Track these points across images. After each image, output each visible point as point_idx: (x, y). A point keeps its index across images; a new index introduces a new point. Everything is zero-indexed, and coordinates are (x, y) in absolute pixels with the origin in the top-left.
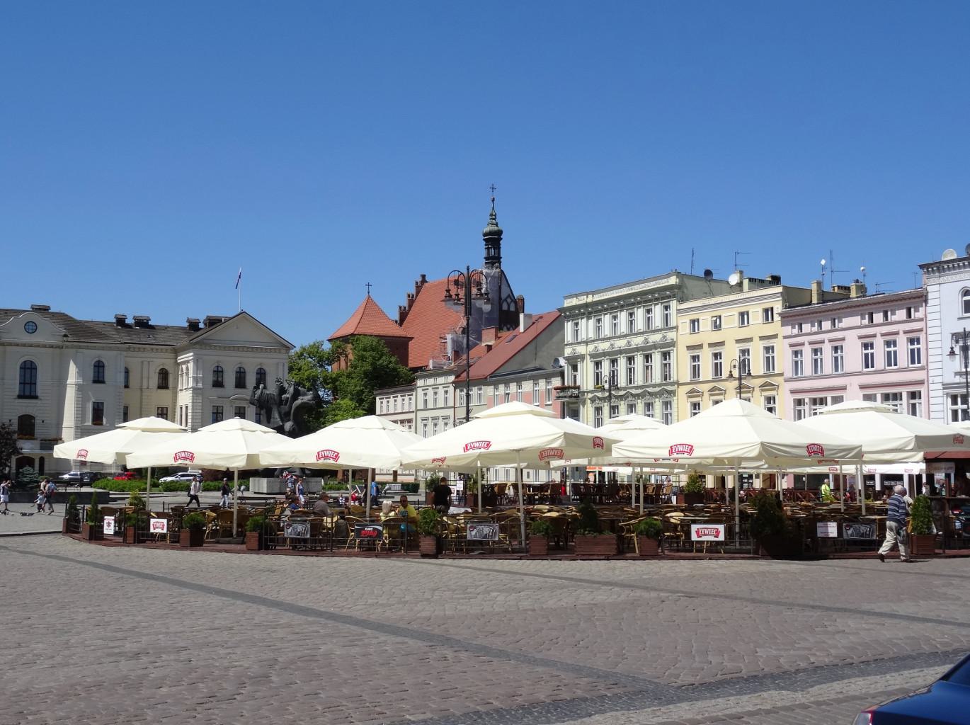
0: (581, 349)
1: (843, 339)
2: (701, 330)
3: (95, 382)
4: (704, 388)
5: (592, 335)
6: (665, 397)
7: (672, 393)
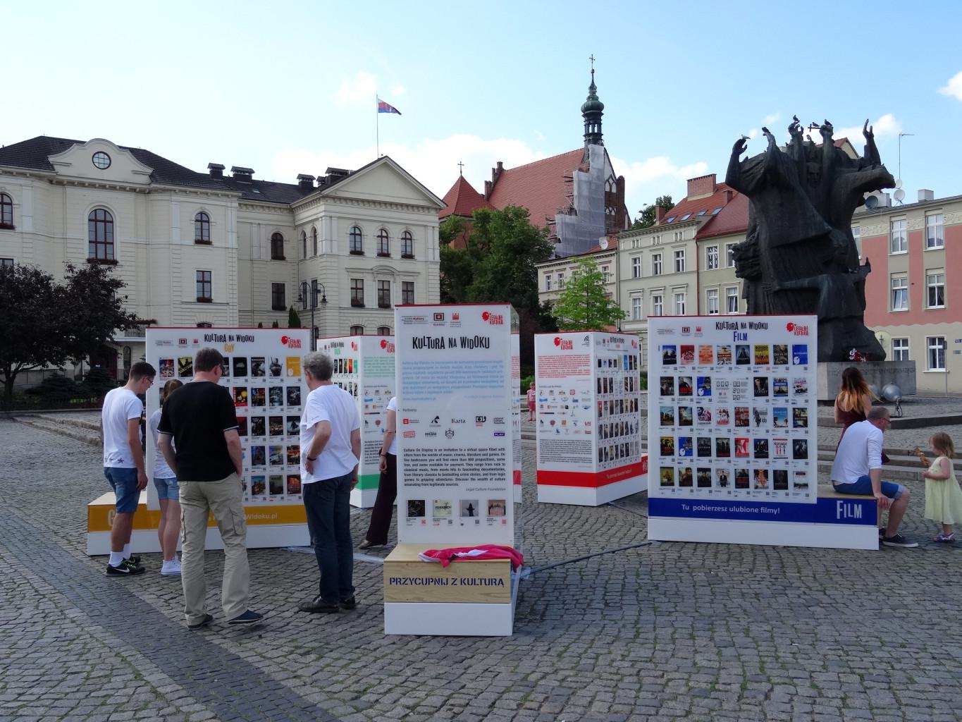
3: (199, 242)
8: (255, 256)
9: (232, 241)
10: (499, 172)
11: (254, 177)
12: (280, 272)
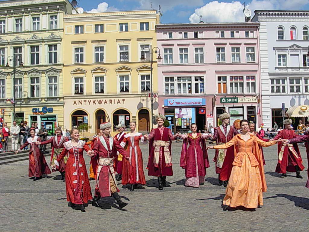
2: (85, 31)
4: (89, 69)
6: (51, 74)
7: (60, 71)
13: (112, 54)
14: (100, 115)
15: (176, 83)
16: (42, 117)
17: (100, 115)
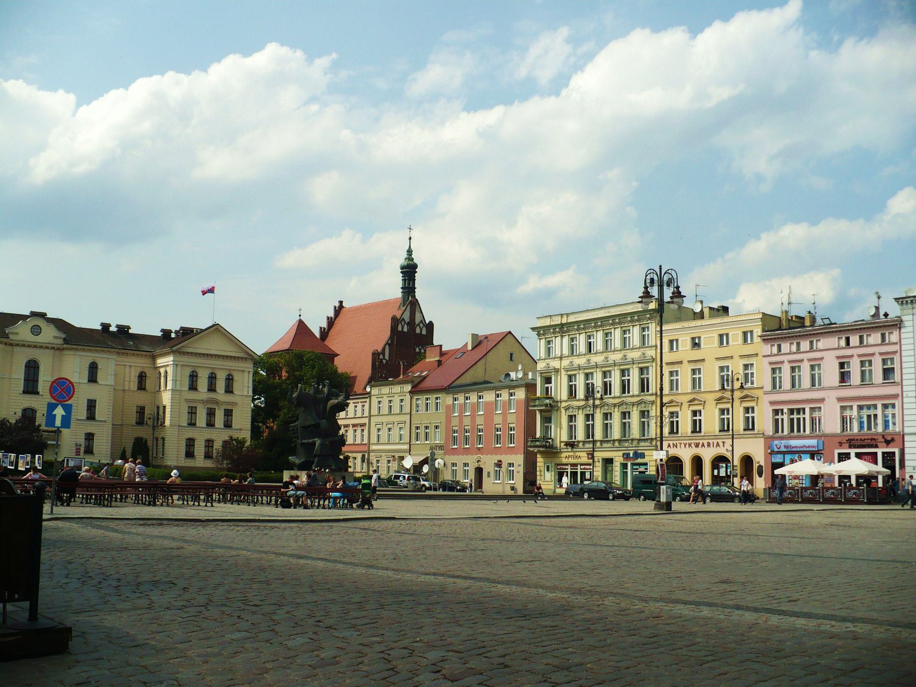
0: (556, 364)
1: (822, 359)
2: (680, 348)
5: (566, 351)
8: (127, 388)
9: (111, 382)
10: (339, 310)
11: (131, 331)
12: (142, 399)
13: (711, 380)
14: (697, 462)
15: (785, 417)
16: (633, 464)
17: (697, 462)
